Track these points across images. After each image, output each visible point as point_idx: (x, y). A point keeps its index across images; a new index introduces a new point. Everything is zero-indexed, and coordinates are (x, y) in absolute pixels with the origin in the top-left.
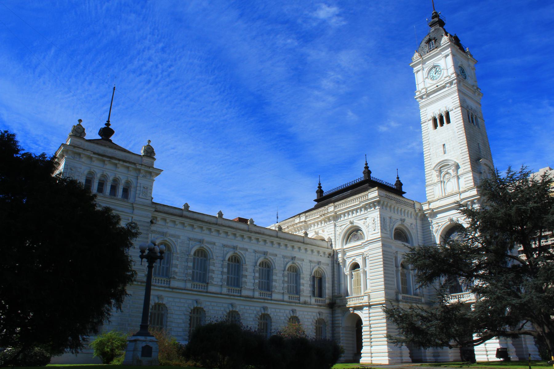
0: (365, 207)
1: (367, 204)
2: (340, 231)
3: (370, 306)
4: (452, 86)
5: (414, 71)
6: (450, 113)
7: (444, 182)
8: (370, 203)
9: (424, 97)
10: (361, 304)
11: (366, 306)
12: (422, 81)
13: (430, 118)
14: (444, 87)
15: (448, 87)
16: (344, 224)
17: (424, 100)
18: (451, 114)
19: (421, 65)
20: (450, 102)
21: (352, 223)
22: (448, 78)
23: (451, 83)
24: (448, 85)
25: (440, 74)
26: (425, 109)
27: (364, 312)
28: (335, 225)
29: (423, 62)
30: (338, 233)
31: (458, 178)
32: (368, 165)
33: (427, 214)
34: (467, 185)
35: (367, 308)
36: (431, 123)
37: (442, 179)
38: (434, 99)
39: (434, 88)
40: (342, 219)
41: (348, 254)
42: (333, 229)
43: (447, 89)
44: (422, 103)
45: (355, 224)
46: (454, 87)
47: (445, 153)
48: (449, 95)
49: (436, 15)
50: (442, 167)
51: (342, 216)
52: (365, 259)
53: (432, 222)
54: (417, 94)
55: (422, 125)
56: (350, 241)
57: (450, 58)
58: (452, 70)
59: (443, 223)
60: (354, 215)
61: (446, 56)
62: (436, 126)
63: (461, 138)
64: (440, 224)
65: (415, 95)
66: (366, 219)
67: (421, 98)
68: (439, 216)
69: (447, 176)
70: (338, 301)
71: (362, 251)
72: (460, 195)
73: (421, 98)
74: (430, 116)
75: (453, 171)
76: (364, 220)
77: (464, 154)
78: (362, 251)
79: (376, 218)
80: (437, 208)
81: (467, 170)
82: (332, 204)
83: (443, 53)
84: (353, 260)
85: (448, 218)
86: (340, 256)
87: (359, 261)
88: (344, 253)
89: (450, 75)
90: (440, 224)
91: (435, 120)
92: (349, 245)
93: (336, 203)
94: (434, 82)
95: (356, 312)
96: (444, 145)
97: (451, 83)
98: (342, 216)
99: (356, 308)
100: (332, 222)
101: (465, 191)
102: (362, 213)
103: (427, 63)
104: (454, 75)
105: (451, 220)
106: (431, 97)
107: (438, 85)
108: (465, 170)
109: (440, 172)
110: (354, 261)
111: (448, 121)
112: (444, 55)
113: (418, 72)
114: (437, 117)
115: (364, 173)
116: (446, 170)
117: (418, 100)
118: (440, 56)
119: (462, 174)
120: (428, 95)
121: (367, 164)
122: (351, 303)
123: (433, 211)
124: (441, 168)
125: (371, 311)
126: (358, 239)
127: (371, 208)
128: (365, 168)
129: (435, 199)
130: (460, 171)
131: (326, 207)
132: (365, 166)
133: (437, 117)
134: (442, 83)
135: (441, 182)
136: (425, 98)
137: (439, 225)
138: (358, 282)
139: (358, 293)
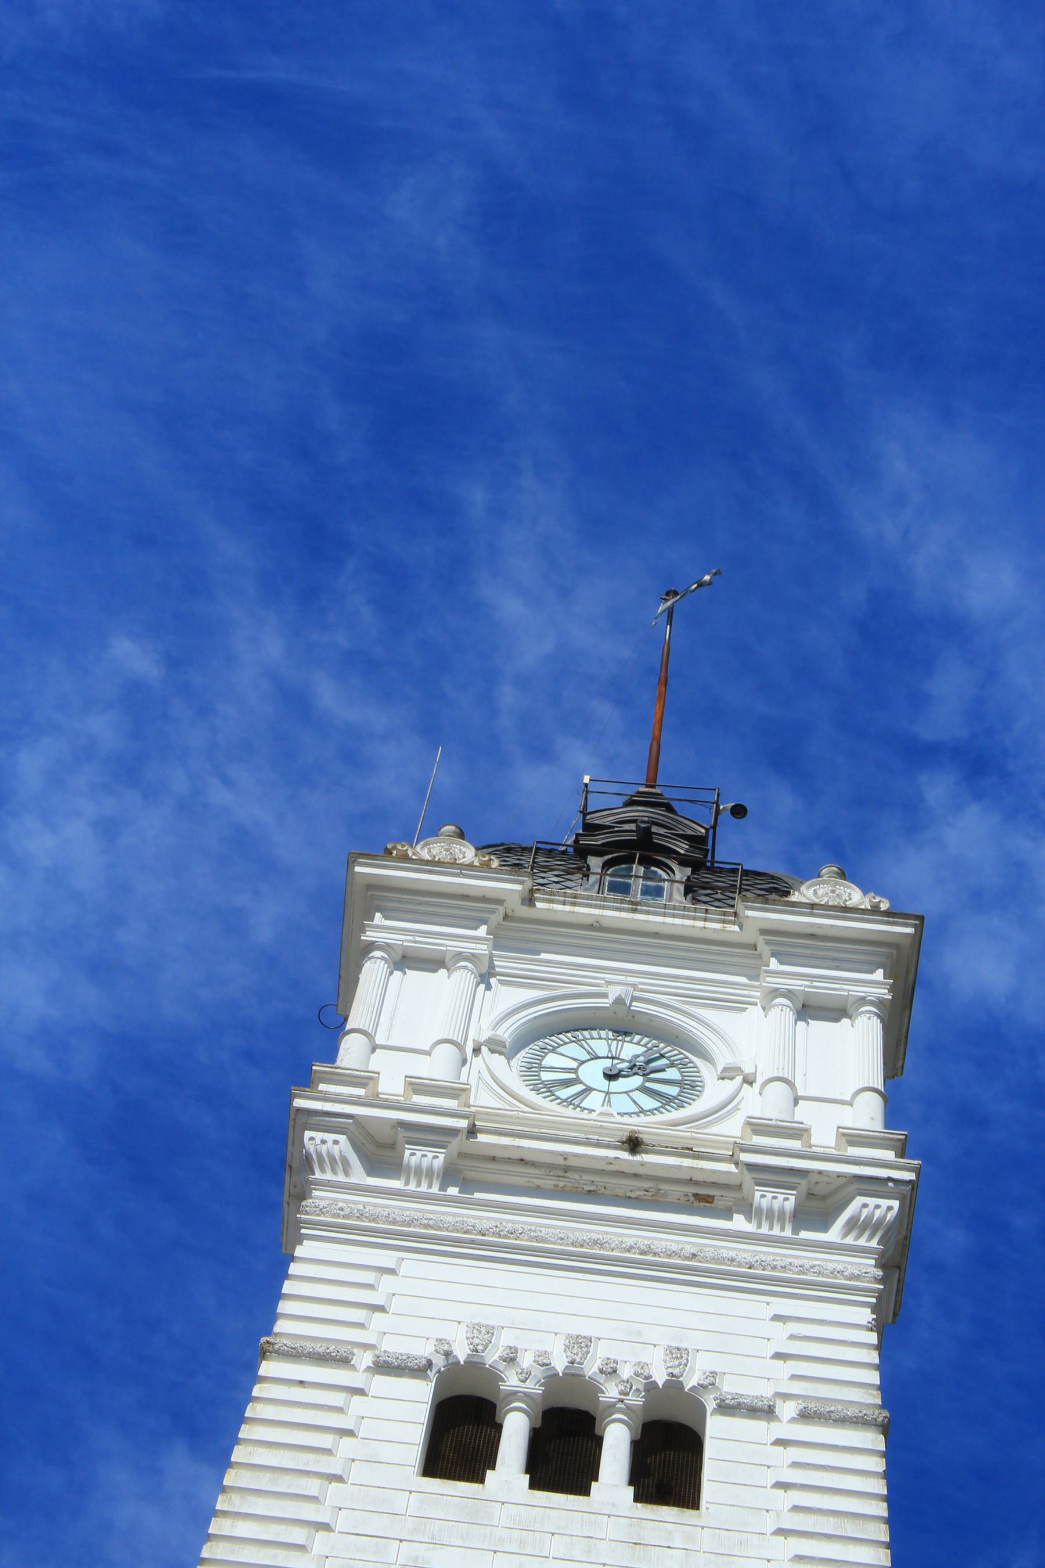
9: (415, 1156)
14: (703, 1197)
18: (721, 1440)
23: (818, 1203)
24: (786, 1201)
36: (406, 1413)
46: (848, 1254)
55: (266, 1368)
65: (306, 1080)
67: (380, 1150)
73: (380, 1150)
97: (818, 1203)
113: (405, 961)
117: (314, 1140)
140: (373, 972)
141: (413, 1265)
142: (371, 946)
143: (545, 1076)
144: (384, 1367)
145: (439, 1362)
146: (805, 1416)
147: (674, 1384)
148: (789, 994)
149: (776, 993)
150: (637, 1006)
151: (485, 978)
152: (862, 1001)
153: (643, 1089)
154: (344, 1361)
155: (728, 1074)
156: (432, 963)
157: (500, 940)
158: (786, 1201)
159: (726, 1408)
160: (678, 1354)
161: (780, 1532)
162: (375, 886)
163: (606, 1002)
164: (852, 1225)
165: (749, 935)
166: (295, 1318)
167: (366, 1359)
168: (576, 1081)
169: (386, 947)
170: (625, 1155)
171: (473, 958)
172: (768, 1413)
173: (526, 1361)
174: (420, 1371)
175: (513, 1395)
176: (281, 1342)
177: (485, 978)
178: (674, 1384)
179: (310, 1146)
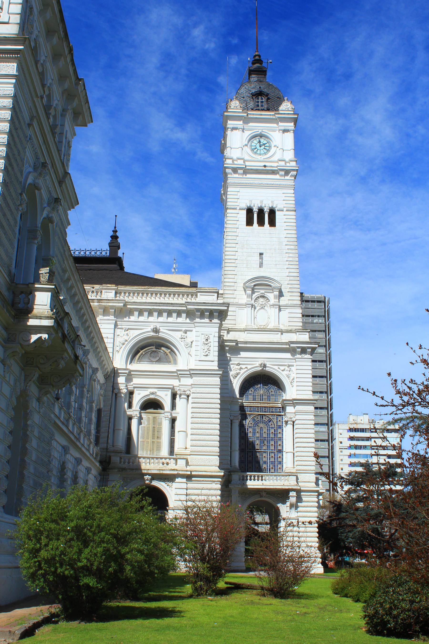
0: (190, 314)
1: (198, 310)
2: (126, 338)
3: (189, 477)
4: (287, 178)
5: (228, 126)
6: (277, 213)
7: (255, 308)
8: (207, 310)
10: (176, 472)
11: (182, 476)
12: (237, 144)
13: (244, 206)
14: (274, 172)
15: (281, 176)
16: (141, 327)
17: (236, 176)
18: (279, 215)
19: (241, 122)
20: (278, 196)
21: (156, 331)
22: (283, 163)
23: (287, 172)
24: (283, 173)
25: (268, 151)
26: (237, 189)
27: (175, 485)
28: (116, 325)
29: (246, 120)
30: (119, 340)
31: (280, 310)
32: (118, 234)
33: (227, 346)
34: (291, 324)
35: (184, 480)
36: (243, 215)
37: (253, 302)
38: (257, 182)
39: (259, 165)
40: (132, 318)
41: (136, 381)
42: (112, 331)
43: (277, 177)
44: (232, 178)
45: (161, 335)
47: (261, 265)
48: (279, 187)
49: (258, 60)
50: (259, 286)
51: (136, 313)
52: (174, 396)
53: (230, 360)
54: (228, 161)
55: (228, 211)
56: (139, 360)
57: (290, 137)
58: (290, 155)
59: (249, 367)
60: (161, 319)
61: (285, 131)
62: (249, 222)
63: (291, 255)
64: (243, 367)
66: (186, 332)
67: (235, 170)
68: (243, 354)
69: (261, 300)
70: (115, 459)
71: (175, 382)
72: (282, 334)
73: (235, 170)
74: (245, 204)
75: (275, 297)
76: (181, 333)
77: (292, 278)
78: (175, 382)
79: (211, 337)
80: (246, 343)
81: (295, 302)
82: (113, 286)
83: (281, 124)
84: (153, 393)
85: (260, 362)
86: (121, 380)
87: (165, 399)
88: (129, 377)
89: (287, 160)
90: (243, 367)
91: (249, 211)
92: (135, 366)
93: (121, 288)
94: (259, 157)
95: (155, 483)
96: (261, 254)
97: (287, 172)
98: (136, 313)
99: (155, 477)
100: (112, 317)
101: (290, 331)
102: (180, 320)
103: (251, 124)
104: (294, 164)
105: (265, 366)
106: (248, 176)
107: (267, 164)
108: (290, 302)
109: (253, 292)
110: (152, 397)
111: (272, 223)
112: (283, 128)
113: (233, 129)
114: (255, 210)
115: (111, 245)
116: (263, 291)
118: (275, 125)
119: (286, 306)
120: (246, 171)
121: (115, 231)
122: (148, 466)
123: (237, 344)
124: (255, 285)
125: (190, 485)
126: (159, 361)
127: (202, 316)
128: (111, 237)
129: (237, 327)
130: (283, 301)
131: (97, 287)
132: (112, 233)
133: (255, 210)
134: (274, 165)
135: (252, 305)
136: (240, 174)
137: (241, 368)
138: (156, 433)
139: (152, 450)
140: (229, 132)
141: (242, 190)
142: (228, 128)
143: (253, 148)
144: (240, 209)
145: (246, 207)
146: (287, 210)
147: (272, 207)
148: (281, 130)
149: (280, 130)
150: (263, 133)
151: (243, 130)
152: (291, 130)
153: (264, 148)
154: (236, 209)
155: (275, 146)
156: (236, 129)
157: (244, 123)
158: (283, 173)
159: (278, 210)
160: (272, 202)
161: (287, 268)
162: (227, 116)
163: (259, 133)
164: (291, 176)
165: (277, 118)
166: (230, 203)
167: (238, 208)
168: (256, 148)
169: (230, 128)
170: (264, 168)
171: (241, 129)
172: (283, 210)
173: (256, 205)
174: (244, 209)
175: (255, 211)
176: (229, 207)
177: (243, 130)
178: (272, 207)
179: (227, 172)
